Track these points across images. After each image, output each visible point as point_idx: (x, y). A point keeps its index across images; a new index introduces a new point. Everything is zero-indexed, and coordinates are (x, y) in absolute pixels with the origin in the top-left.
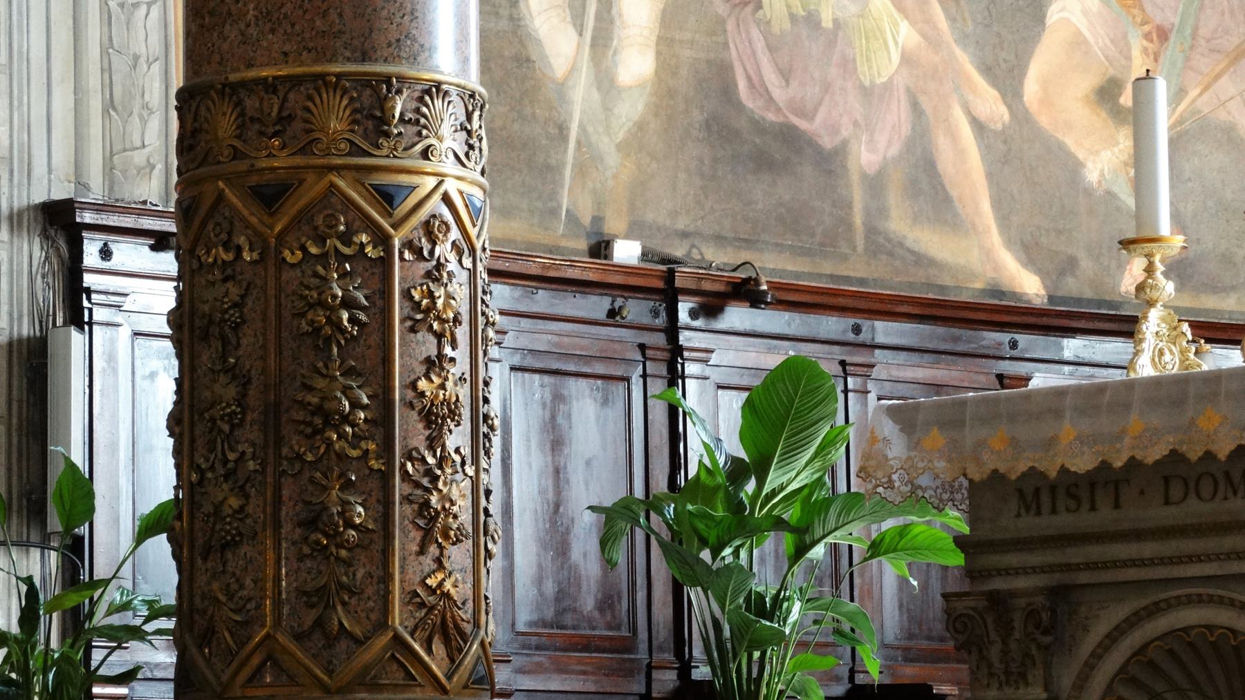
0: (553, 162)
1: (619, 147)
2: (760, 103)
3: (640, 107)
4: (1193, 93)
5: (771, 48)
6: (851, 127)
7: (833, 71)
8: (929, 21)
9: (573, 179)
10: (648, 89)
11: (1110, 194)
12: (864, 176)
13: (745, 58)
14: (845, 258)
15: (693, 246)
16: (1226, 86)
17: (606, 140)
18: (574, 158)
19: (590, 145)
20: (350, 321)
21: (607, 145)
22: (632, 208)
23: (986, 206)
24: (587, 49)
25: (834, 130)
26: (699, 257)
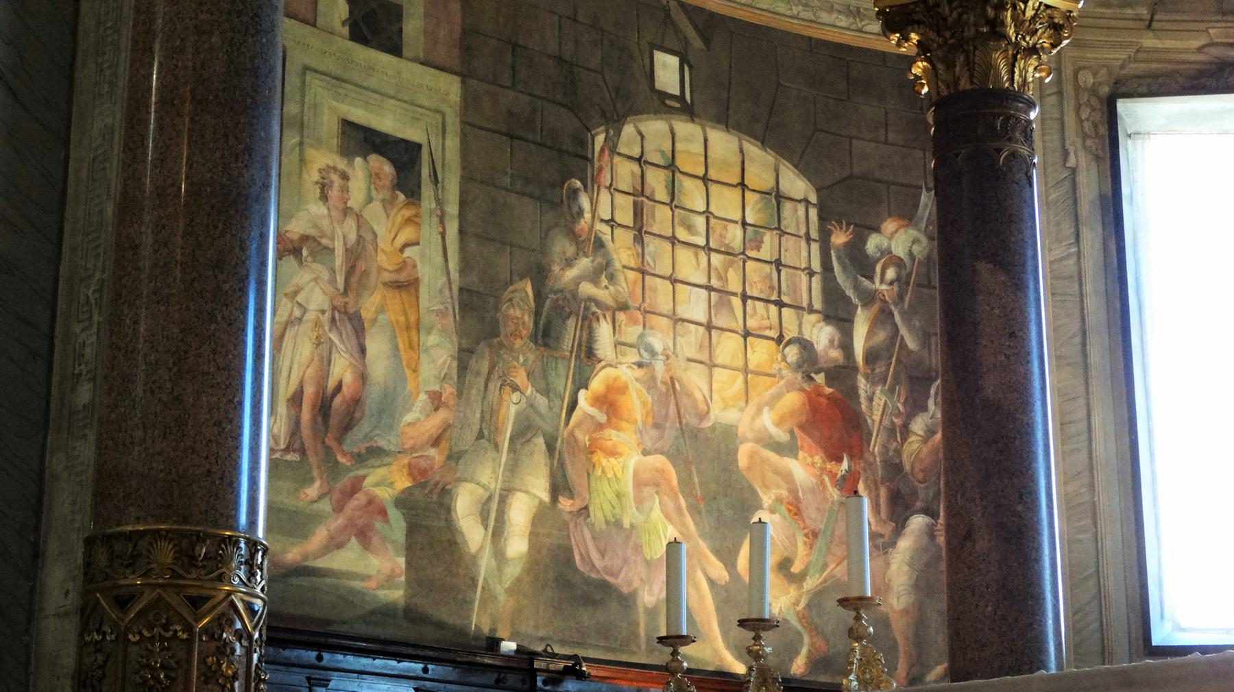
0: (468, 599)
1: (506, 591)
4: (832, 566)
5: (594, 538)
6: (639, 582)
7: (629, 551)
8: (684, 525)
9: (480, 609)
11: (786, 621)
12: (646, 608)
14: (634, 653)
15: (548, 645)
17: (499, 586)
20: (165, 677)
22: (513, 624)
24: (490, 537)
25: (630, 583)
26: (551, 651)
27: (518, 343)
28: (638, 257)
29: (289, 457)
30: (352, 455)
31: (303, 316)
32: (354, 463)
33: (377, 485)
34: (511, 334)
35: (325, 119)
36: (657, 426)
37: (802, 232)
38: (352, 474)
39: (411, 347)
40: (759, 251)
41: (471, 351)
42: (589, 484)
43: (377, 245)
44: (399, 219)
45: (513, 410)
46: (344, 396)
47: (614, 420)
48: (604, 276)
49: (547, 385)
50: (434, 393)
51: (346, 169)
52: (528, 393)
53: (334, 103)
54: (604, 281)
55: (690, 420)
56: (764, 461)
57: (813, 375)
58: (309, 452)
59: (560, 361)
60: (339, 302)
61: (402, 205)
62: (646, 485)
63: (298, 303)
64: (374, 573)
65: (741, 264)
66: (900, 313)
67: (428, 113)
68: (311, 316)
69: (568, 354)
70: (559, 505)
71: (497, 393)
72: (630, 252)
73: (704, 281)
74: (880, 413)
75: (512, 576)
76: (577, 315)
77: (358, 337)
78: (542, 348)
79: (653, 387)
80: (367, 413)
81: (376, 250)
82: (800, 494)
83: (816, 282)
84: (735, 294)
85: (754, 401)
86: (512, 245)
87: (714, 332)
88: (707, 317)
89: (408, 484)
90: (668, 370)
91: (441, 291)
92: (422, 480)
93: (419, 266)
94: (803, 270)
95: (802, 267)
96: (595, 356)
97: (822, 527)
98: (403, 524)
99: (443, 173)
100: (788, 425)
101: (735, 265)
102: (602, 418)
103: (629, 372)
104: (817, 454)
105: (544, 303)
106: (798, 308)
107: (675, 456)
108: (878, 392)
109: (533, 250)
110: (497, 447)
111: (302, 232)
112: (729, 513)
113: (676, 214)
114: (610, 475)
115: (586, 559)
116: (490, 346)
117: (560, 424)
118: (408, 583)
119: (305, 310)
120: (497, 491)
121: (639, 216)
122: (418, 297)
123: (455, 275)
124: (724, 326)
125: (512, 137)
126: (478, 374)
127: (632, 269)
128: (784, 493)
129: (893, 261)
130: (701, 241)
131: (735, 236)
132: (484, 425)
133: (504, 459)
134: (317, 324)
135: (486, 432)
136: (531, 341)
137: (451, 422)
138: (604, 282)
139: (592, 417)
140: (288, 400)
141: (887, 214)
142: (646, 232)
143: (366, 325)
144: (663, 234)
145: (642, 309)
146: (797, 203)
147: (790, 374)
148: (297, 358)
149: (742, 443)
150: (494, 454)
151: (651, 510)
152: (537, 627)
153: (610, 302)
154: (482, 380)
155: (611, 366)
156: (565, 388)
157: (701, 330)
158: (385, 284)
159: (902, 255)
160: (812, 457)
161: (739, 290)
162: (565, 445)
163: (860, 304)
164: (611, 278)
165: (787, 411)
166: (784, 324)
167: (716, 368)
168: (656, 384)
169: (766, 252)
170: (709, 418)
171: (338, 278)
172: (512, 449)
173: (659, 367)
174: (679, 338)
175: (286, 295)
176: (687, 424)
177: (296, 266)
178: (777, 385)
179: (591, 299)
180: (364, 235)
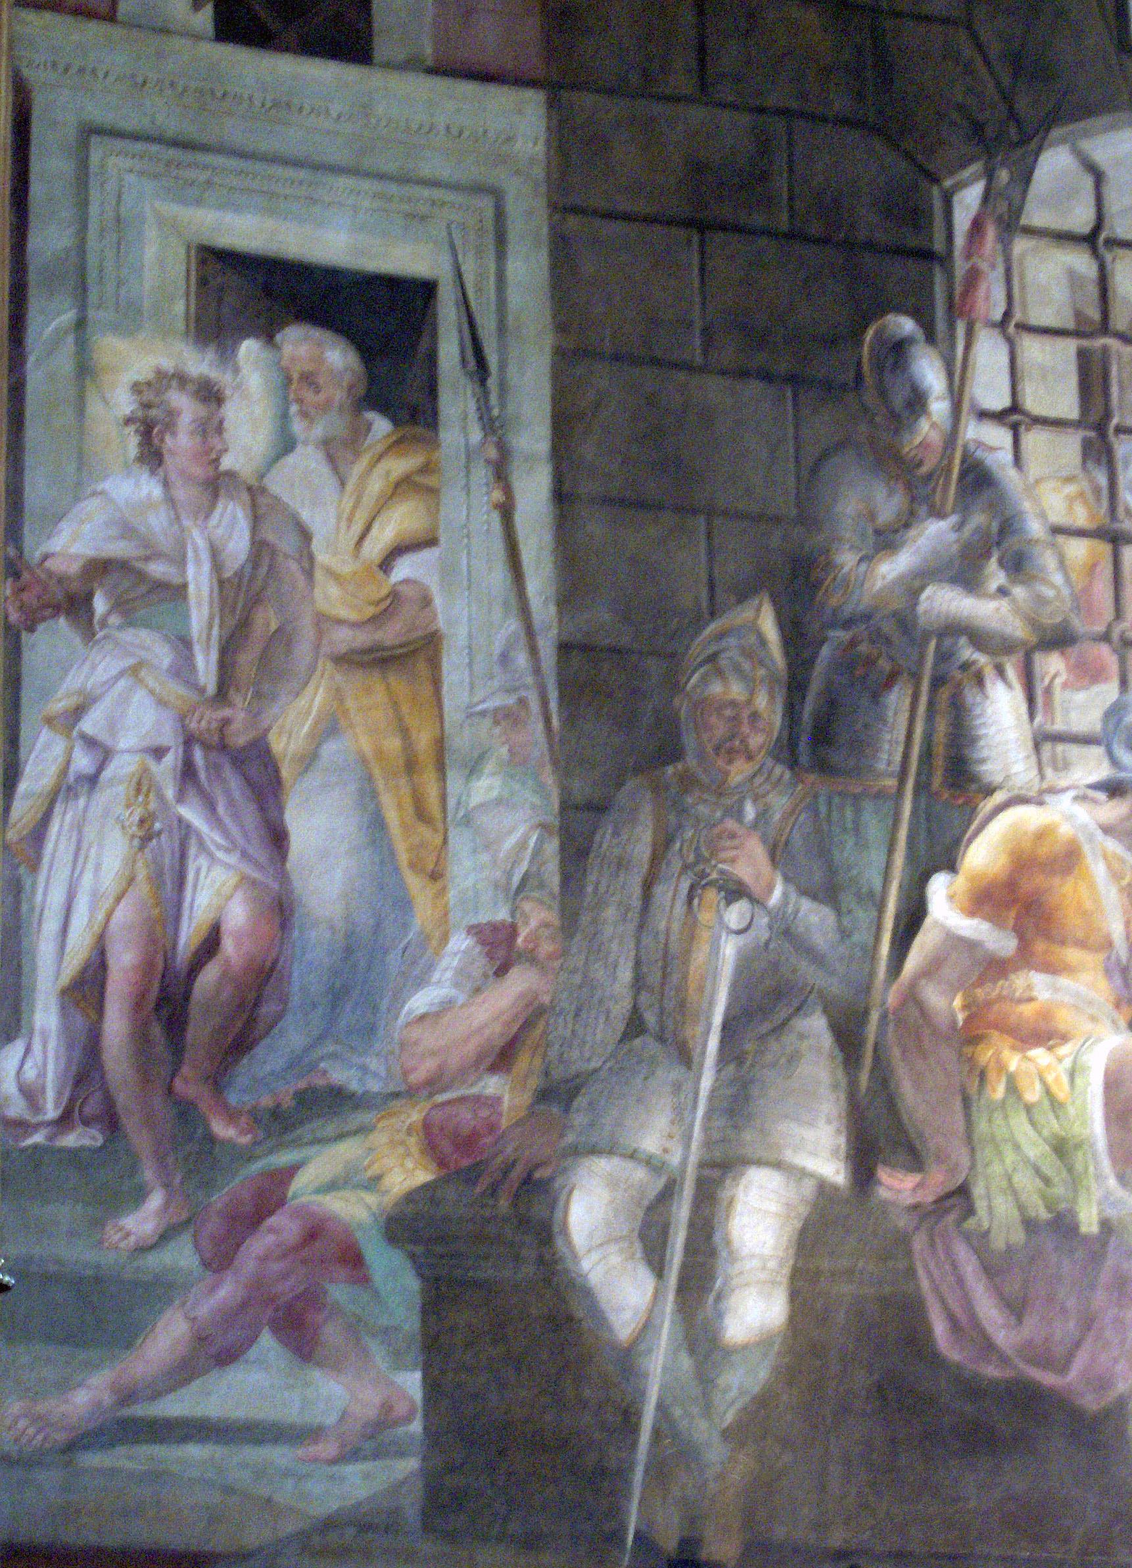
0: (612, 1464)
1: (726, 1434)
3: (763, 1374)
9: (645, 1486)
13: (944, 1288)
17: (703, 1425)
18: (649, 1452)
19: (676, 1435)
22: (748, 1519)
24: (671, 1297)
25: (1103, 1383)
28: (1098, 499)
29: (71, 1140)
30: (255, 1116)
31: (100, 769)
32: (261, 1135)
33: (332, 1186)
35: (150, 252)
38: (256, 1167)
39: (421, 814)
41: (598, 808)
43: (311, 558)
44: (376, 486)
45: (729, 949)
46: (227, 961)
47: (1040, 946)
48: (993, 561)
49: (831, 869)
50: (495, 927)
51: (214, 375)
53: (172, 209)
54: (996, 576)
58: (131, 1123)
59: (868, 806)
60: (205, 721)
61: (380, 448)
63: (84, 737)
64: (331, 1420)
67: (450, 196)
68: (123, 766)
69: (891, 783)
71: (680, 909)
72: (1071, 489)
75: (742, 1392)
76: (916, 677)
77: (262, 809)
78: (811, 777)
80: (295, 1000)
81: (309, 574)
86: (711, 512)
89: (423, 1176)
91: (505, 659)
92: (465, 1163)
93: (438, 601)
96: (974, 778)
98: (412, 1283)
99: (503, 349)
102: (1001, 942)
103: (1083, 815)
105: (815, 656)
109: (777, 519)
110: (685, 1056)
111: (91, 553)
114: (1033, 1094)
116: (658, 789)
117: (872, 974)
118: (433, 1436)
119: (103, 752)
121: (1097, 389)
122: (436, 683)
125: (702, 227)
126: (622, 864)
127: (1081, 533)
132: (644, 998)
133: (707, 1082)
134: (142, 785)
135: (651, 1019)
136: (778, 760)
137: (546, 999)
138: (996, 576)
139: (970, 945)
140: (64, 992)
142: (1119, 430)
143: (285, 773)
145: (1115, 636)
148: (87, 880)
150: (677, 1073)
153: (1017, 629)
154: (634, 883)
155: (1020, 800)
158: (347, 660)
162: (891, 1028)
171: (200, 660)
175: (49, 721)
177: (78, 641)
179: (955, 629)
180: (271, 537)
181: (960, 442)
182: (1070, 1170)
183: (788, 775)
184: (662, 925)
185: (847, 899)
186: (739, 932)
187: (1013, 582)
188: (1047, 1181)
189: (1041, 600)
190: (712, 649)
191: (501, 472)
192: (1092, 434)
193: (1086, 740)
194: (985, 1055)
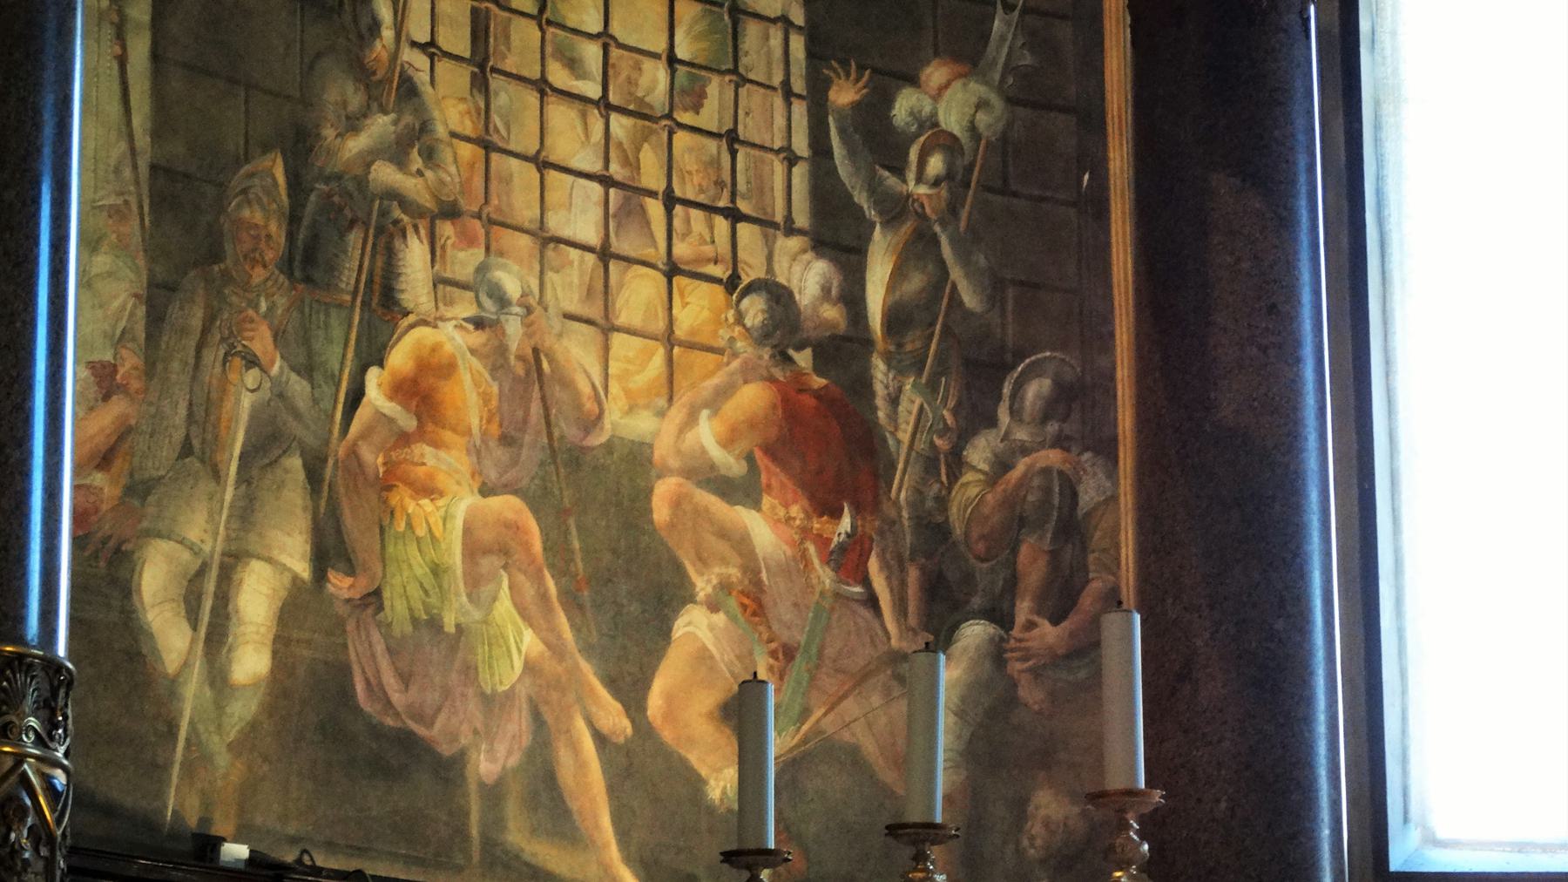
0: (160, 761)
1: (230, 746)
2: (379, 707)
4: (818, 713)
5: (389, 650)
6: (471, 737)
8: (553, 629)
9: (181, 778)
10: (262, 689)
12: (482, 785)
13: (364, 660)
15: (305, 851)
16: (850, 707)
17: (216, 739)
18: (183, 755)
19: (200, 743)
21: (217, 745)
22: (242, 810)
23: (606, 821)
24: (201, 645)
26: (309, 863)
27: (258, 275)
28: (479, 114)
34: (245, 257)
36: (506, 440)
37: (777, 79)
40: (698, 113)
41: (171, 288)
42: (383, 547)
45: (247, 401)
47: (430, 427)
48: (415, 151)
49: (310, 354)
50: (103, 365)
52: (275, 370)
54: (417, 162)
55: (567, 429)
56: (701, 513)
57: (791, 352)
59: (334, 312)
62: (487, 551)
65: (665, 135)
66: (952, 241)
69: (348, 298)
70: (329, 586)
71: (218, 365)
72: (462, 107)
73: (596, 167)
74: (910, 429)
75: (241, 719)
76: (366, 225)
78: (301, 287)
79: (502, 366)
82: (764, 575)
83: (800, 173)
84: (652, 194)
85: (684, 399)
87: (612, 266)
88: (602, 234)
90: (528, 335)
91: (117, 171)
94: (778, 152)
95: (776, 147)
96: (397, 303)
97: (802, 639)
100: (743, 445)
101: (654, 138)
103: (459, 338)
104: (795, 501)
105: (306, 199)
106: (765, 223)
107: (537, 501)
108: (908, 387)
109: (288, 97)
110: (217, 475)
112: (635, 608)
113: (548, 36)
114: (421, 531)
115: (377, 690)
117: (330, 432)
120: (217, 557)
121: (482, 34)
123: (143, 141)
124: (633, 254)
126: (184, 331)
127: (467, 139)
128: (734, 573)
129: (941, 141)
130: (592, 90)
131: (655, 81)
132: (194, 428)
133: (229, 495)
135: (196, 443)
136: (282, 272)
137: (133, 422)
138: (417, 162)
139: (391, 421)
141: (931, 51)
142: (494, 70)
144: (525, 73)
145: (484, 216)
146: (767, 24)
147: (750, 350)
149: (659, 477)
150: (212, 485)
151: (495, 599)
152: (284, 818)
153: (426, 201)
154: (192, 343)
155: (424, 323)
156: (342, 364)
157: (590, 259)
159: (957, 131)
160: (786, 506)
161: (659, 185)
162: (340, 473)
163: (877, 219)
164: (429, 155)
165: (742, 418)
166: (741, 254)
167: (616, 334)
168: (506, 359)
169: (710, 115)
170: (602, 429)
172: (244, 478)
173: (513, 328)
174: (550, 276)
176: (562, 437)
178: (727, 369)
181: (399, 62)
182: (440, 587)
183: (287, 283)
184: (207, 379)
185: (318, 377)
186: (253, 391)
187: (427, 167)
188: (426, 592)
189: (442, 182)
190: (248, 183)
191: (120, 37)
192: (476, 70)
193: (464, 286)
194: (394, 499)
